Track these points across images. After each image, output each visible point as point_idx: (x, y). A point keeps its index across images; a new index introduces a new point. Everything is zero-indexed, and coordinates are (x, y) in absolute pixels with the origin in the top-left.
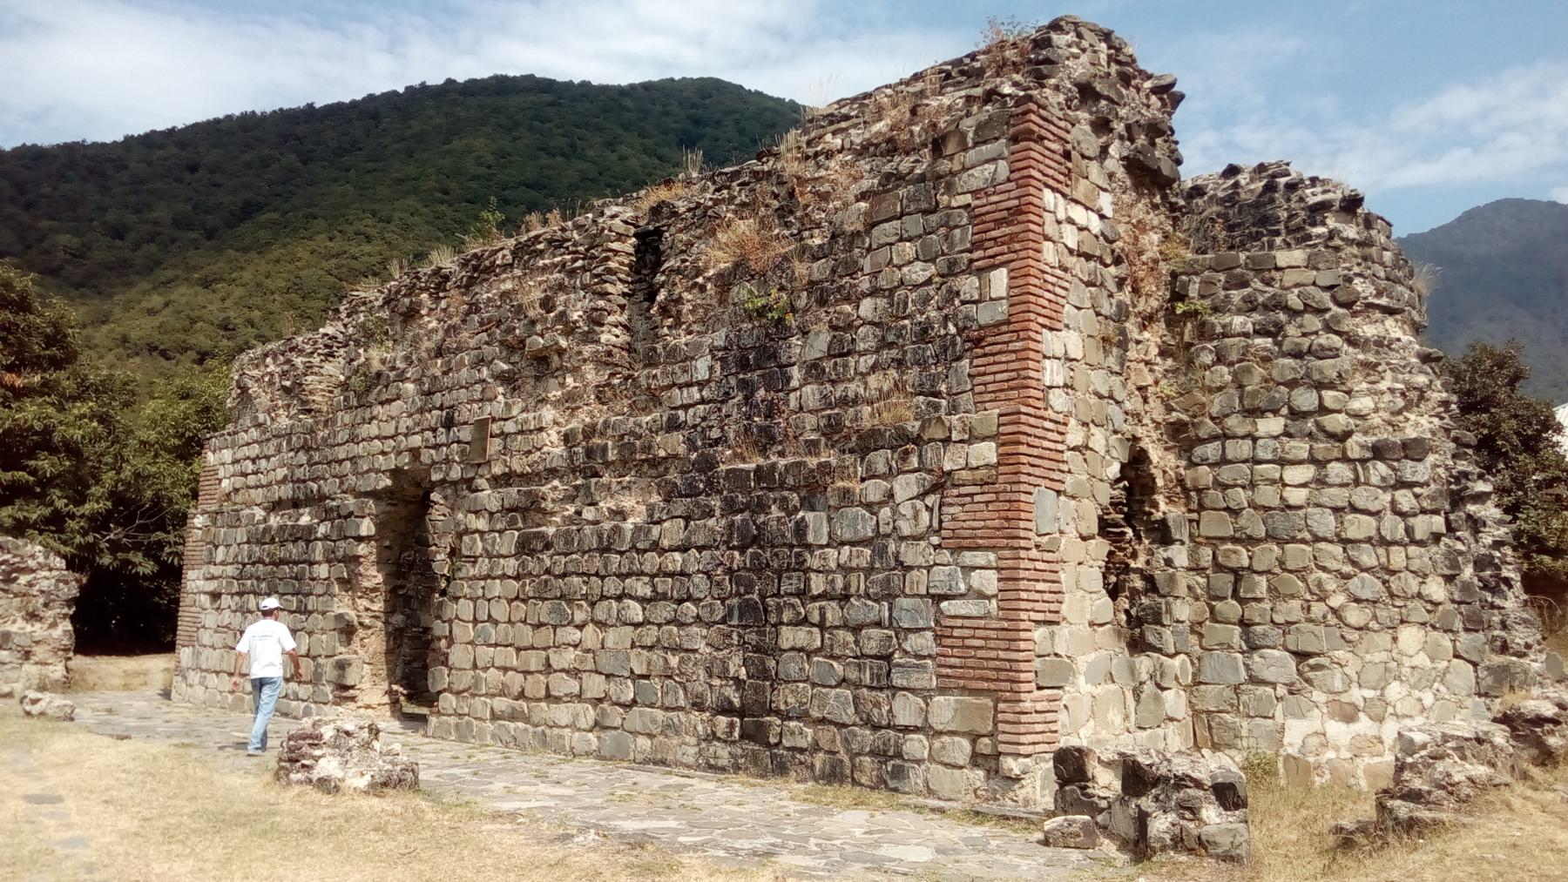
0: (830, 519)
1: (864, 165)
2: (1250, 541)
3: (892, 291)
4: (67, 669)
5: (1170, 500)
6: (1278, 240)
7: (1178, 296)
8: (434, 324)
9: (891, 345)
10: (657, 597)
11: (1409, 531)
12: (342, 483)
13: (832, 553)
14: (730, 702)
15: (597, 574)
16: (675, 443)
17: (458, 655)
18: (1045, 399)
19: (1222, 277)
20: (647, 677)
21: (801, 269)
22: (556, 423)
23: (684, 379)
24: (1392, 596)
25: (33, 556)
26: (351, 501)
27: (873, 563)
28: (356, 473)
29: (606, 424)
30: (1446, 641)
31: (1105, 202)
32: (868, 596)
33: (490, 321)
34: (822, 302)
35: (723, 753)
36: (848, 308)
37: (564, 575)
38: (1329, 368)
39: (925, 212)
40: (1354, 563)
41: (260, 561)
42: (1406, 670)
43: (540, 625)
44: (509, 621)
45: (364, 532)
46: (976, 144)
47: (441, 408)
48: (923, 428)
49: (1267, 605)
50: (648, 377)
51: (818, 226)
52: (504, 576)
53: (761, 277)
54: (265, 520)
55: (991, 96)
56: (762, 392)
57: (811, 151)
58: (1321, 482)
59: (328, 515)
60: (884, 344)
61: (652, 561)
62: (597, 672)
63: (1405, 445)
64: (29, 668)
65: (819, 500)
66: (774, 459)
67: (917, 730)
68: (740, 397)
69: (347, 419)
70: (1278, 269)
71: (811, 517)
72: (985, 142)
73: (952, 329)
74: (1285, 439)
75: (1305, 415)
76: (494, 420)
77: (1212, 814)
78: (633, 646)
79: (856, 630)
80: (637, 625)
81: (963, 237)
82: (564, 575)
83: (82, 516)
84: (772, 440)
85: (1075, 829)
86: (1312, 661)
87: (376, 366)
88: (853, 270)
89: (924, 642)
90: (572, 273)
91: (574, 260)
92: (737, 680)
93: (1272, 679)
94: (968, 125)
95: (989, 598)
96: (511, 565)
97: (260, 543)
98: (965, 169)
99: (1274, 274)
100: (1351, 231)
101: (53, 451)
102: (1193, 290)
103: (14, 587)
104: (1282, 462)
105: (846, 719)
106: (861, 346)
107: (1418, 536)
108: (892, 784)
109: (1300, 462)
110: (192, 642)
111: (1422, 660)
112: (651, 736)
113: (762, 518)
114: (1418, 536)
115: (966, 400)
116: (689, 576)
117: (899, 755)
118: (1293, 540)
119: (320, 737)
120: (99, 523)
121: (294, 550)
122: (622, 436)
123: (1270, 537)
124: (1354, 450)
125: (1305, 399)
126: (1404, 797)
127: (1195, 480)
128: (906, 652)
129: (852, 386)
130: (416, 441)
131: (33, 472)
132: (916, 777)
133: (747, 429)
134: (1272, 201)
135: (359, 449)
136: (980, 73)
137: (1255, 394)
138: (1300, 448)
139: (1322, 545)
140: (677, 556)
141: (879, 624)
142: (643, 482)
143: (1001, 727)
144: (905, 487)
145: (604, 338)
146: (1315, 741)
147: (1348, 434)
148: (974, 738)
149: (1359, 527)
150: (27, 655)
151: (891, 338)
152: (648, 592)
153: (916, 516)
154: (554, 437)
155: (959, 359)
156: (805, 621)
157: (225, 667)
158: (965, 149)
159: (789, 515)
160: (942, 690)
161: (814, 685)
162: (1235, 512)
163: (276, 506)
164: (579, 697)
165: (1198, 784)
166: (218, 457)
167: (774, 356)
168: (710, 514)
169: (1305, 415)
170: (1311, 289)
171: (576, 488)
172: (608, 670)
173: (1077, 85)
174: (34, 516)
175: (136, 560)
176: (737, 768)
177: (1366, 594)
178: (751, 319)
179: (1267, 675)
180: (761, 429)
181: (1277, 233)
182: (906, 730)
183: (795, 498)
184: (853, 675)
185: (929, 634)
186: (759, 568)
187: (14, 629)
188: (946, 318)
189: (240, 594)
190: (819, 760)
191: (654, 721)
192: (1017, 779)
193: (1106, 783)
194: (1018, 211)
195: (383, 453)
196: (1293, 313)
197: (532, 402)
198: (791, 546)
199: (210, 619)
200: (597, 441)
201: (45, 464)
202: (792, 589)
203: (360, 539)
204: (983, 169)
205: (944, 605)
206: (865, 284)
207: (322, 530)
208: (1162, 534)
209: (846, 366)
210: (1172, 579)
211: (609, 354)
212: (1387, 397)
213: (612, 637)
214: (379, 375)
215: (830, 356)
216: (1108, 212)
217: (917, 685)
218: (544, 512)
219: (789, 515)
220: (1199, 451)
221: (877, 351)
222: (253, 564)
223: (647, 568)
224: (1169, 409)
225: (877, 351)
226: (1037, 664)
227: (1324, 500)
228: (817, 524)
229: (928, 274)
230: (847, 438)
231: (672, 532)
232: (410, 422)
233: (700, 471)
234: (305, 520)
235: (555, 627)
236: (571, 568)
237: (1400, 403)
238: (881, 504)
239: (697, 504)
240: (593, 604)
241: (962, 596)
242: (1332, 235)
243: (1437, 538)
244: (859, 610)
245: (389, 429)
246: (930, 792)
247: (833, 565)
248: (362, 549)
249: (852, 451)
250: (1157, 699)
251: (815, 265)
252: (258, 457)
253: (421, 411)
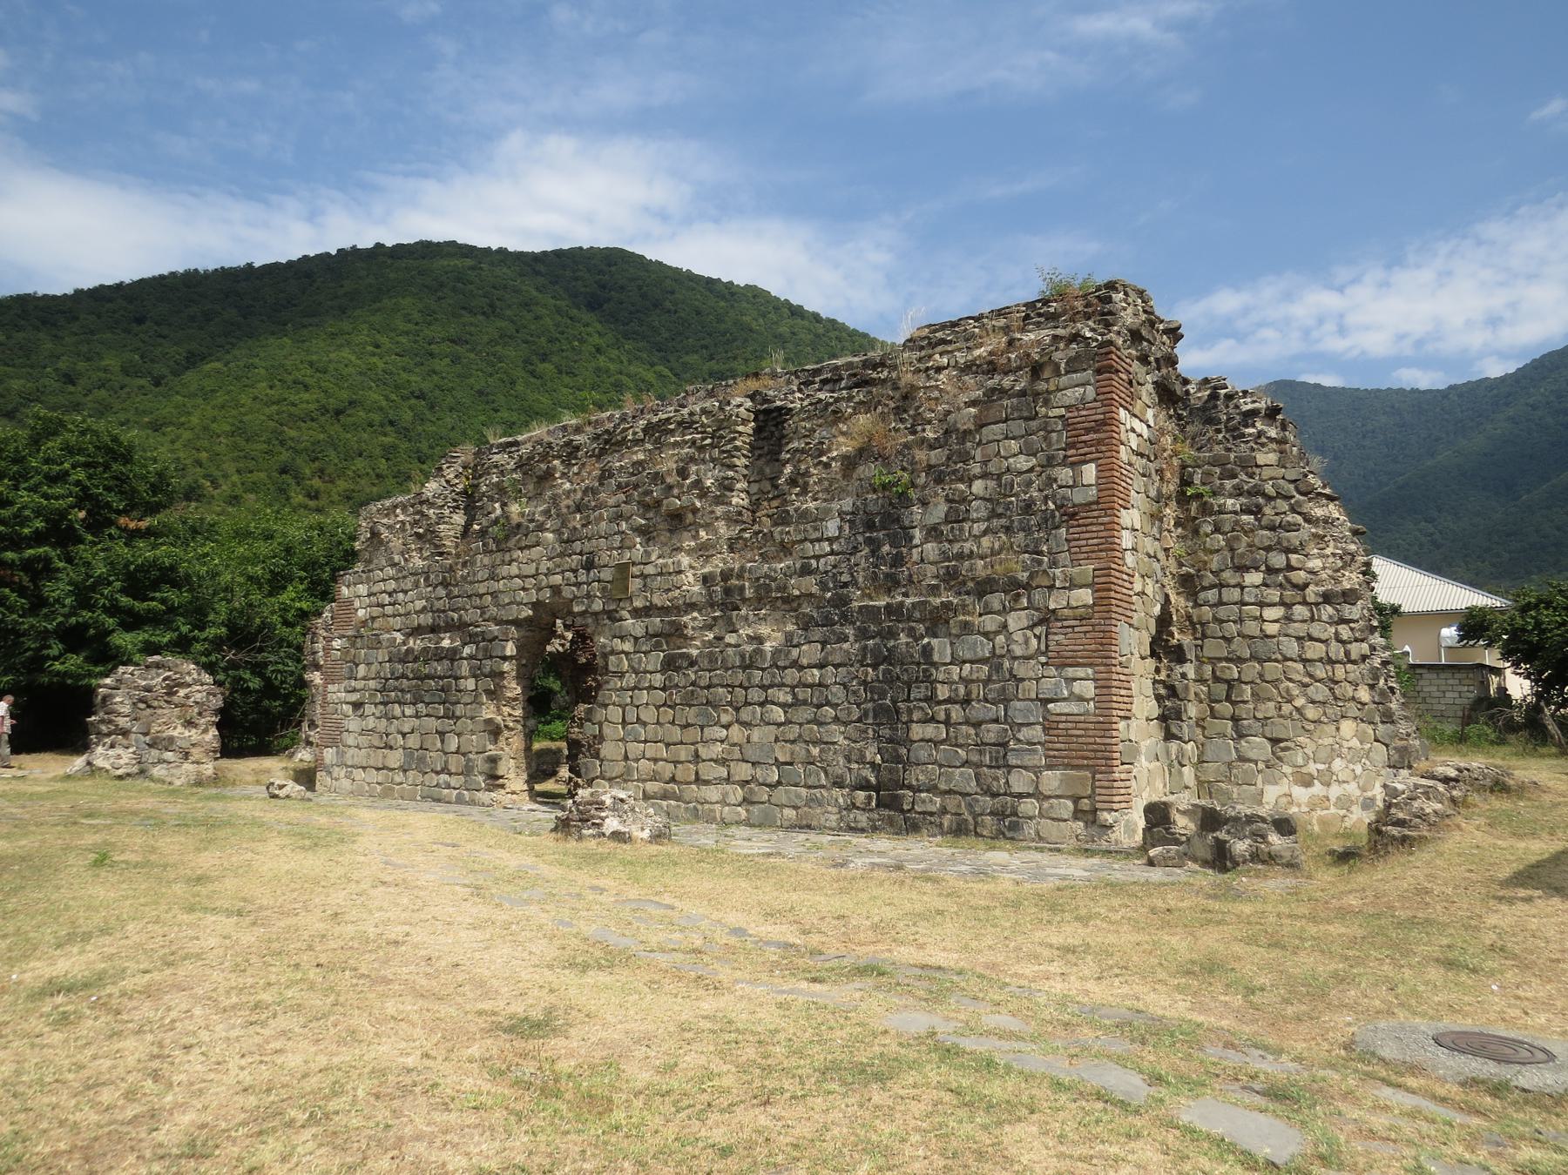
0: (952, 644)
1: (969, 380)
2: (1239, 660)
3: (999, 476)
5: (1181, 631)
6: (1220, 436)
7: (1186, 482)
8: (567, 486)
9: (1000, 516)
10: (798, 703)
11: (1347, 653)
12: (483, 613)
13: (956, 669)
14: (868, 781)
15: (740, 686)
16: (810, 584)
17: (607, 750)
18: (1123, 559)
19: (1218, 470)
20: (791, 764)
21: (921, 455)
22: (691, 567)
23: (817, 535)
24: (1336, 698)
25: (189, 673)
26: (494, 628)
27: (990, 676)
28: (497, 605)
29: (742, 568)
30: (1369, 729)
31: (1150, 414)
32: (986, 700)
33: (627, 485)
34: (939, 481)
35: (863, 819)
36: (962, 487)
37: (708, 687)
38: (1294, 538)
39: (1027, 419)
40: (1311, 676)
41: (404, 676)
42: (1345, 750)
43: (688, 725)
44: (658, 723)
45: (508, 653)
46: (1067, 372)
47: (581, 554)
48: (1031, 577)
50: (781, 533)
51: (929, 422)
52: (651, 688)
53: (883, 458)
54: (404, 643)
55: (1075, 337)
56: (886, 548)
57: (922, 366)
58: (1288, 619)
59: (472, 639)
60: (993, 515)
61: (791, 675)
62: (743, 761)
63: (1344, 593)
64: (187, 766)
65: (942, 629)
66: (900, 599)
67: (1029, 795)
68: (867, 550)
69: (486, 561)
70: (1257, 466)
71: (935, 642)
72: (1075, 372)
73: (1052, 506)
75: (1278, 571)
76: (634, 564)
77: (1274, 838)
78: (777, 740)
79: (977, 725)
80: (779, 725)
81: (1059, 439)
82: (708, 687)
84: (897, 584)
85: (1172, 854)
87: (515, 519)
88: (966, 458)
89: (1036, 733)
90: (702, 449)
91: (703, 439)
92: (873, 764)
94: (1057, 356)
95: (1087, 701)
96: (658, 679)
97: (403, 661)
98: (1059, 390)
99: (1257, 471)
100: (1273, 433)
101: (176, 585)
102: (1197, 479)
104: (1262, 604)
105: (969, 790)
106: (975, 515)
107: (1353, 657)
108: (1009, 834)
109: (1274, 605)
111: (1355, 743)
112: (795, 808)
113: (892, 643)
114: (1353, 657)
115: (1064, 558)
116: (827, 687)
117: (1015, 814)
118: (1269, 660)
119: (603, 803)
120: (217, 644)
121: (439, 668)
122: (758, 579)
123: (1253, 657)
124: (1311, 598)
125: (1278, 560)
126: (1393, 824)
127: (1199, 616)
128: (1019, 741)
129: (967, 545)
130: (557, 579)
131: (163, 601)
132: (1029, 829)
133: (875, 577)
134: (1216, 407)
135: (495, 586)
136: (1053, 317)
137: (1242, 556)
138: (1274, 595)
139: (1289, 663)
140: (815, 671)
141: (996, 721)
142: (778, 615)
143: (1098, 791)
144: (1017, 621)
145: (735, 501)
146: (1284, 800)
147: (1306, 585)
148: (1076, 800)
149: (1314, 650)
150: (186, 755)
151: (1000, 510)
152: (789, 699)
153: (1027, 642)
154: (691, 579)
155: (1058, 527)
156: (933, 720)
157: (372, 763)
158: (1059, 375)
159: (916, 640)
160: (1049, 767)
161: (941, 766)
162: (1228, 640)
163: (416, 631)
164: (728, 780)
165: (1264, 820)
166: (353, 591)
167: (898, 520)
168: (846, 640)
169: (1278, 571)
170: (1281, 482)
171: (715, 619)
172: (753, 759)
173: (1130, 331)
174: (165, 640)
176: (875, 829)
177: (1319, 698)
178: (875, 491)
179: (1252, 755)
180: (887, 575)
181: (1218, 431)
182: (1020, 796)
183: (921, 628)
184: (975, 758)
185: (1039, 727)
186: (890, 680)
187: (175, 733)
188: (1046, 498)
189: (385, 704)
190: (947, 820)
191: (798, 796)
192: (1111, 827)
193: (1183, 825)
194: (1104, 423)
195: (524, 589)
196: (1269, 498)
197: (667, 550)
198: (918, 664)
199: (354, 724)
200: (734, 582)
201: (173, 596)
202: (921, 696)
203: (505, 658)
204: (1075, 391)
205: (1050, 706)
206: (976, 469)
207: (467, 651)
208: (1178, 655)
209: (961, 530)
210: (1187, 688)
211: (740, 513)
212: (1331, 559)
213: (756, 734)
214: (519, 525)
215: (947, 522)
216: (1151, 423)
217: (1030, 763)
218: (686, 637)
219: (916, 640)
220: (1202, 595)
221: (988, 519)
222: (397, 679)
223: (788, 681)
224: (1181, 565)
225: (988, 519)
226: (1120, 747)
227: (1290, 631)
228: (941, 648)
229: (1030, 464)
230: (964, 583)
231: (809, 652)
232: (550, 564)
233: (836, 607)
234: (446, 643)
235: (702, 728)
236: (715, 681)
237: (1340, 563)
238: (997, 633)
239: (834, 632)
240: (737, 709)
241: (1065, 700)
242: (1260, 434)
243: (1364, 658)
244: (978, 710)
245: (531, 569)
246: (1041, 839)
247: (956, 678)
248: (506, 666)
249: (968, 593)
250: (1180, 773)
251: (933, 453)
252: (395, 591)
253: (562, 555)
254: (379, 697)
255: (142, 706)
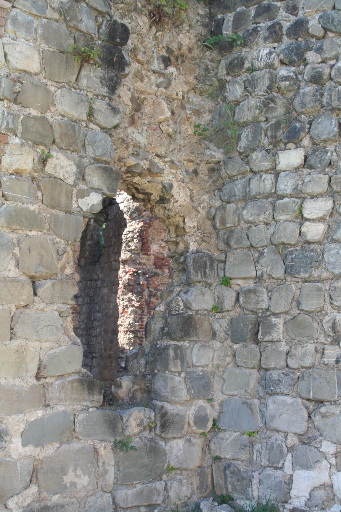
49: (284, 347)
74: (306, 171)
86: (323, 410)
93: (284, 428)
109: (321, 195)
146: (321, 494)
179: (276, 424)
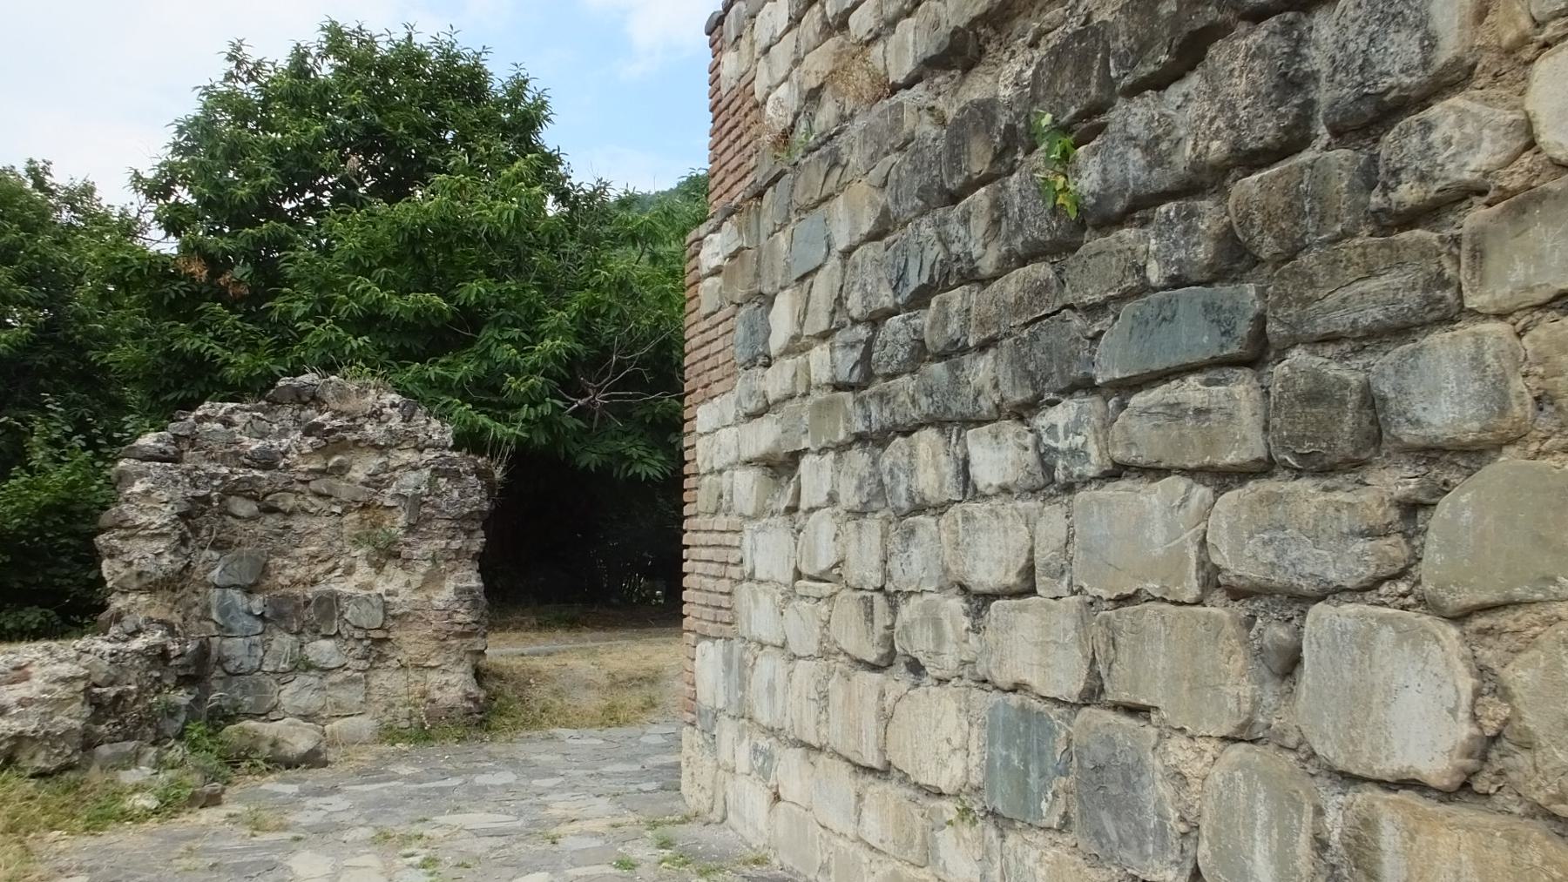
4: (479, 675)
25: (376, 415)
83: (534, 370)
103: (343, 489)
110: (726, 624)
175: (634, 452)
187: (347, 587)
199: (768, 551)
222: (920, 299)
254: (852, 417)
255: (243, 507)
